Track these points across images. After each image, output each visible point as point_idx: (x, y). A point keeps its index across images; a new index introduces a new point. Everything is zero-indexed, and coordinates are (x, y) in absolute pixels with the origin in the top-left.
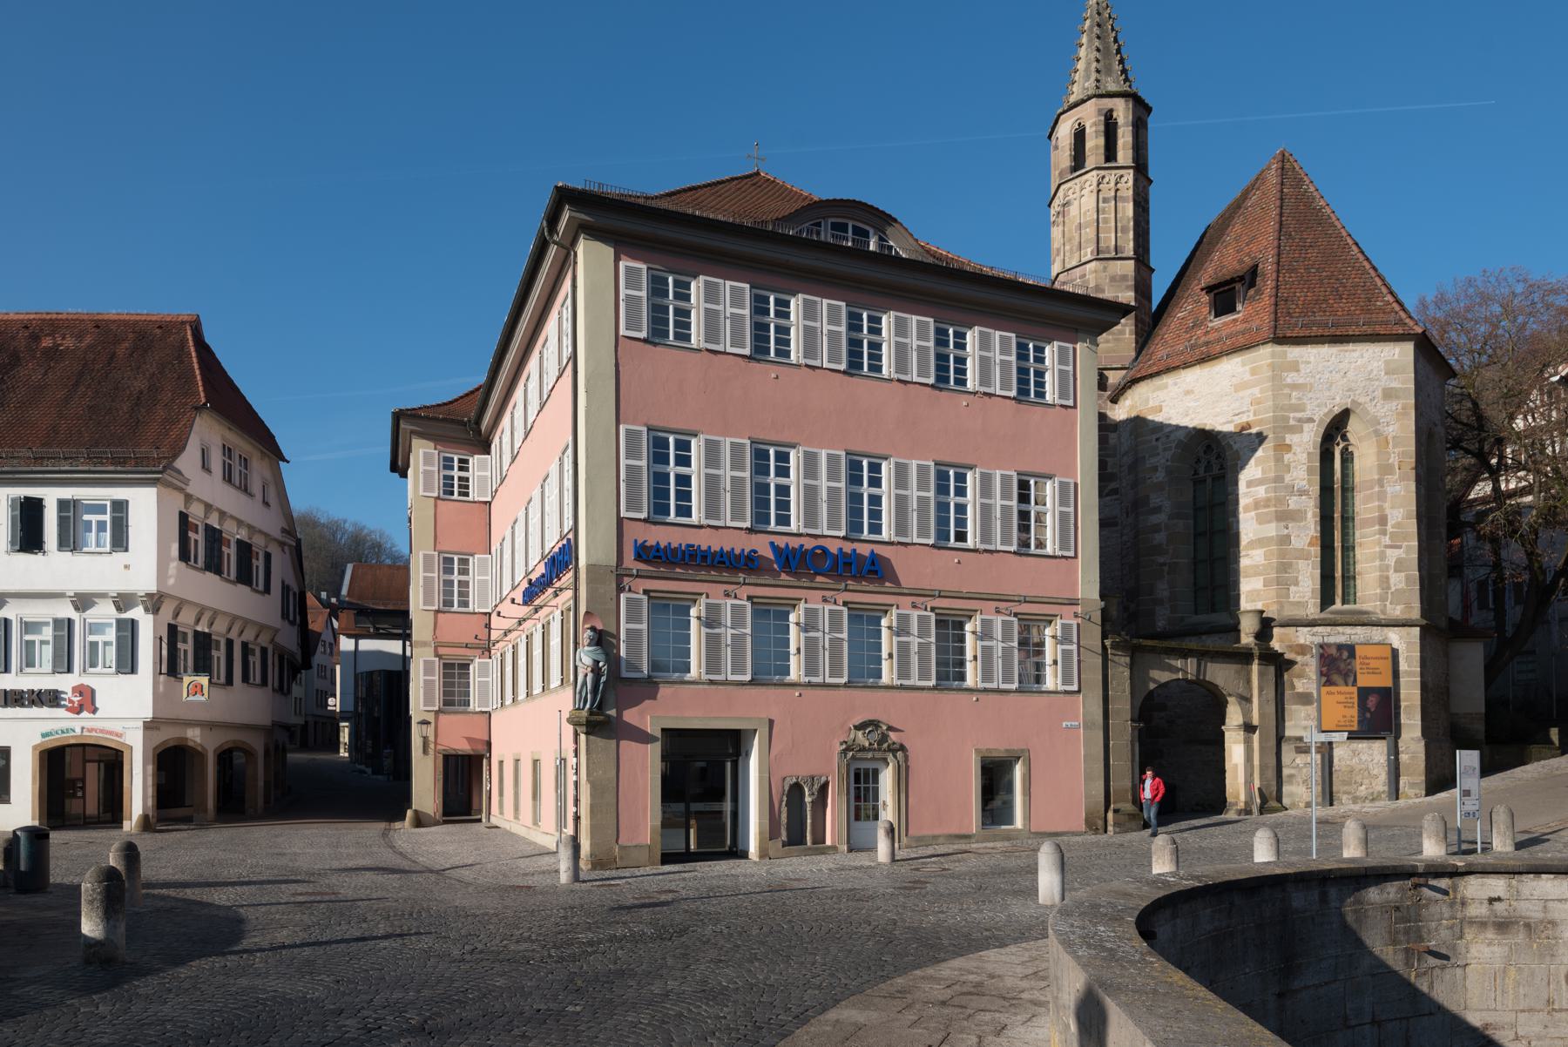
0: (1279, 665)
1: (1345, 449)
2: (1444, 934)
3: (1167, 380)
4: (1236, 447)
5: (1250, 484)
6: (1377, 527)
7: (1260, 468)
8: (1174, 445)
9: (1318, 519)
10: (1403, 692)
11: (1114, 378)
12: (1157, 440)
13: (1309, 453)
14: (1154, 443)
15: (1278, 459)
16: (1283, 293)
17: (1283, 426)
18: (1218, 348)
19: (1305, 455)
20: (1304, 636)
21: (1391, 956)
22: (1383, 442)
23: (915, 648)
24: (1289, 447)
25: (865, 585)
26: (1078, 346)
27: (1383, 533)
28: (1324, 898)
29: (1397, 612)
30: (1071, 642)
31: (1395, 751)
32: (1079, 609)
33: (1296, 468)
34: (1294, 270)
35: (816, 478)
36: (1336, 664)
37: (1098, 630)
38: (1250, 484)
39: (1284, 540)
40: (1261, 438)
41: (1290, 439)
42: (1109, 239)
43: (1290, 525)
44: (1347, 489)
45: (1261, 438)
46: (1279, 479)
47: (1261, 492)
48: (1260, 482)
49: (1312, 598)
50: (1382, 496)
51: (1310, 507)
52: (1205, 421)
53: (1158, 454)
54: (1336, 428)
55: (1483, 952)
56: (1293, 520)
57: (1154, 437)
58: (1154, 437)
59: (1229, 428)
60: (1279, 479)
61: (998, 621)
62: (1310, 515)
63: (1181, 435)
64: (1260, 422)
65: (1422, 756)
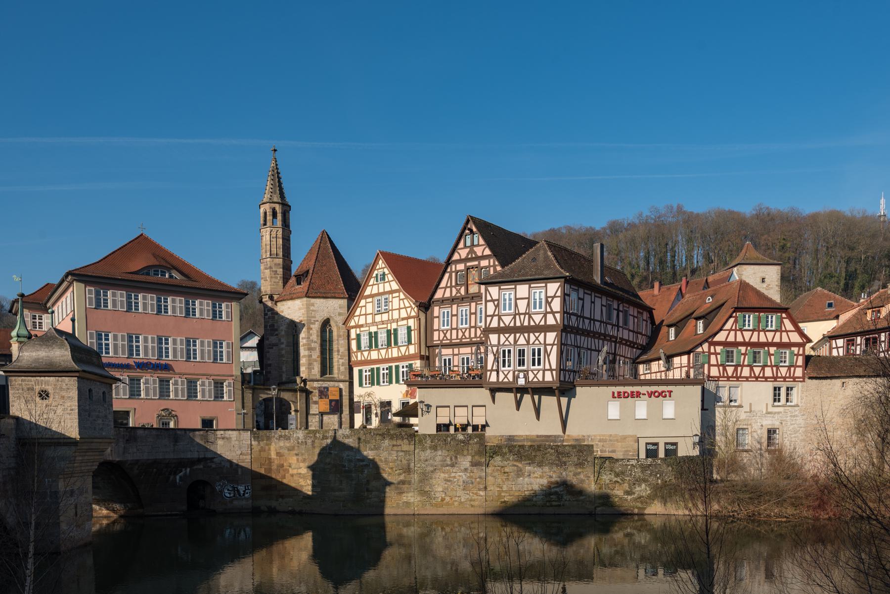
0: (307, 393)
1: (330, 329)
2: (213, 439)
3: (284, 303)
5: (302, 338)
10: (344, 401)
11: (275, 297)
15: (308, 332)
16: (313, 281)
17: (310, 322)
18: (295, 296)
20: (316, 384)
21: (202, 443)
22: (338, 328)
23: (180, 389)
25: (164, 372)
26: (233, 303)
28: (185, 433)
29: (342, 377)
30: (231, 387)
31: (340, 418)
32: (234, 378)
34: (316, 274)
35: (147, 343)
36: (323, 393)
37: (240, 384)
38: (302, 338)
39: (310, 356)
40: (304, 325)
41: (312, 326)
42: (274, 251)
44: (331, 341)
45: (304, 325)
46: (308, 338)
50: (338, 344)
51: (317, 346)
54: (326, 323)
55: (220, 442)
59: (298, 321)
60: (308, 338)
61: (207, 382)
63: (287, 321)
64: (304, 320)
65: (349, 419)
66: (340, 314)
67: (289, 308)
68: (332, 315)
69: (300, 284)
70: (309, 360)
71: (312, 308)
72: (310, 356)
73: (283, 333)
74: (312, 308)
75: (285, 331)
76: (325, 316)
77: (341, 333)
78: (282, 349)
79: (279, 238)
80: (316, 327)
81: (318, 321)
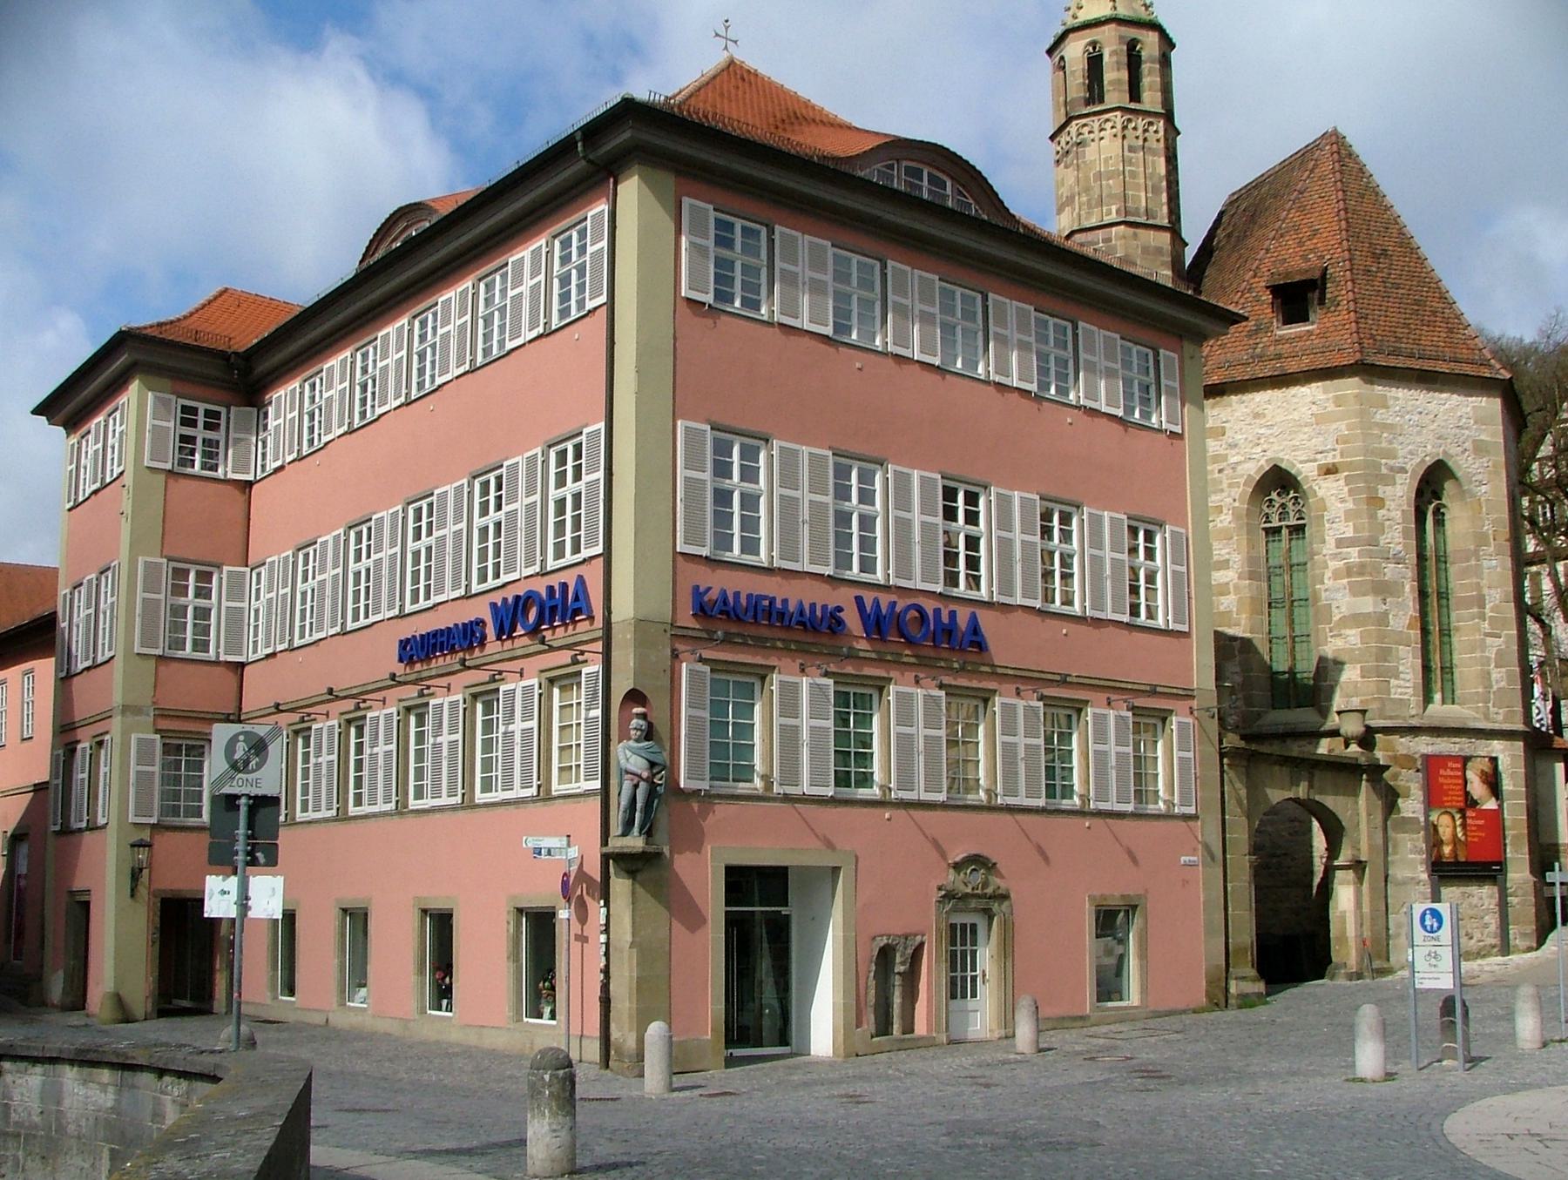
4: (1320, 493)
6: (1476, 610)
7: (1351, 524)
8: (1242, 481)
9: (1416, 596)
12: (1220, 471)
13: (1403, 511)
14: (1217, 475)
15: (1373, 516)
19: (1399, 513)
24: (1382, 499)
27: (1482, 617)
33: (1390, 527)
38: (1340, 543)
43: (1388, 600)
44: (1442, 559)
47: (1354, 554)
48: (1351, 542)
49: (1414, 695)
51: (1404, 576)
52: (1281, 455)
53: (1222, 491)
56: (1392, 595)
57: (1217, 467)
58: (1217, 467)
60: (1372, 541)
62: (1407, 588)
66: (1480, 449)
67: (1257, 416)
68: (1453, 451)
69: (1304, 319)
70: (1381, 637)
71: (1380, 416)
72: (1382, 619)
73: (1224, 520)
74: (1380, 416)
75: (1236, 515)
76: (1429, 453)
77: (1488, 528)
78: (1223, 590)
79: (1154, 153)
80: (1400, 494)
81: (1403, 470)
